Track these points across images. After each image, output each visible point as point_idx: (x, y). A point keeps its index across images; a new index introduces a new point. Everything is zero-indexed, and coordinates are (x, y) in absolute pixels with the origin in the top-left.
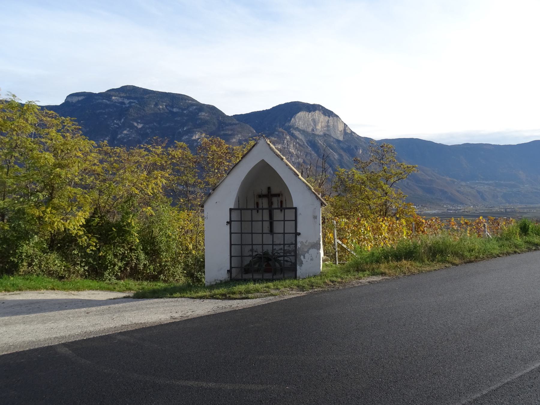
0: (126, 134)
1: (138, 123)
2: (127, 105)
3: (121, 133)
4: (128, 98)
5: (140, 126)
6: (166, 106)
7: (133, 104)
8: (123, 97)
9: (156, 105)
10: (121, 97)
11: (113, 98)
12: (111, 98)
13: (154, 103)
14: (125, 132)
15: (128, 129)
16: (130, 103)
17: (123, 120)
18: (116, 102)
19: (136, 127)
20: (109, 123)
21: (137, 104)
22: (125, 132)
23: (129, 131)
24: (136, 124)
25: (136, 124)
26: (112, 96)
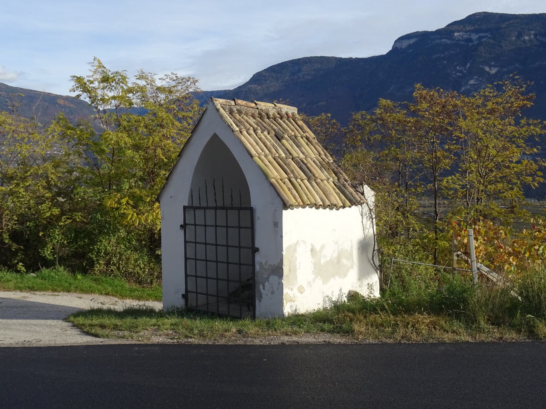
0: (474, 85)
1: (490, 66)
2: (476, 43)
3: (467, 84)
4: (476, 31)
5: (494, 71)
6: (535, 35)
7: (484, 40)
8: (470, 31)
9: (520, 35)
10: (466, 32)
11: (456, 34)
12: (453, 35)
13: (516, 33)
14: (472, 82)
15: (476, 77)
16: (480, 38)
17: (468, 65)
18: (458, 40)
19: (488, 73)
20: (449, 71)
21: (489, 38)
22: (472, 82)
23: (477, 80)
24: (487, 69)
25: (487, 69)
26: (454, 32)
